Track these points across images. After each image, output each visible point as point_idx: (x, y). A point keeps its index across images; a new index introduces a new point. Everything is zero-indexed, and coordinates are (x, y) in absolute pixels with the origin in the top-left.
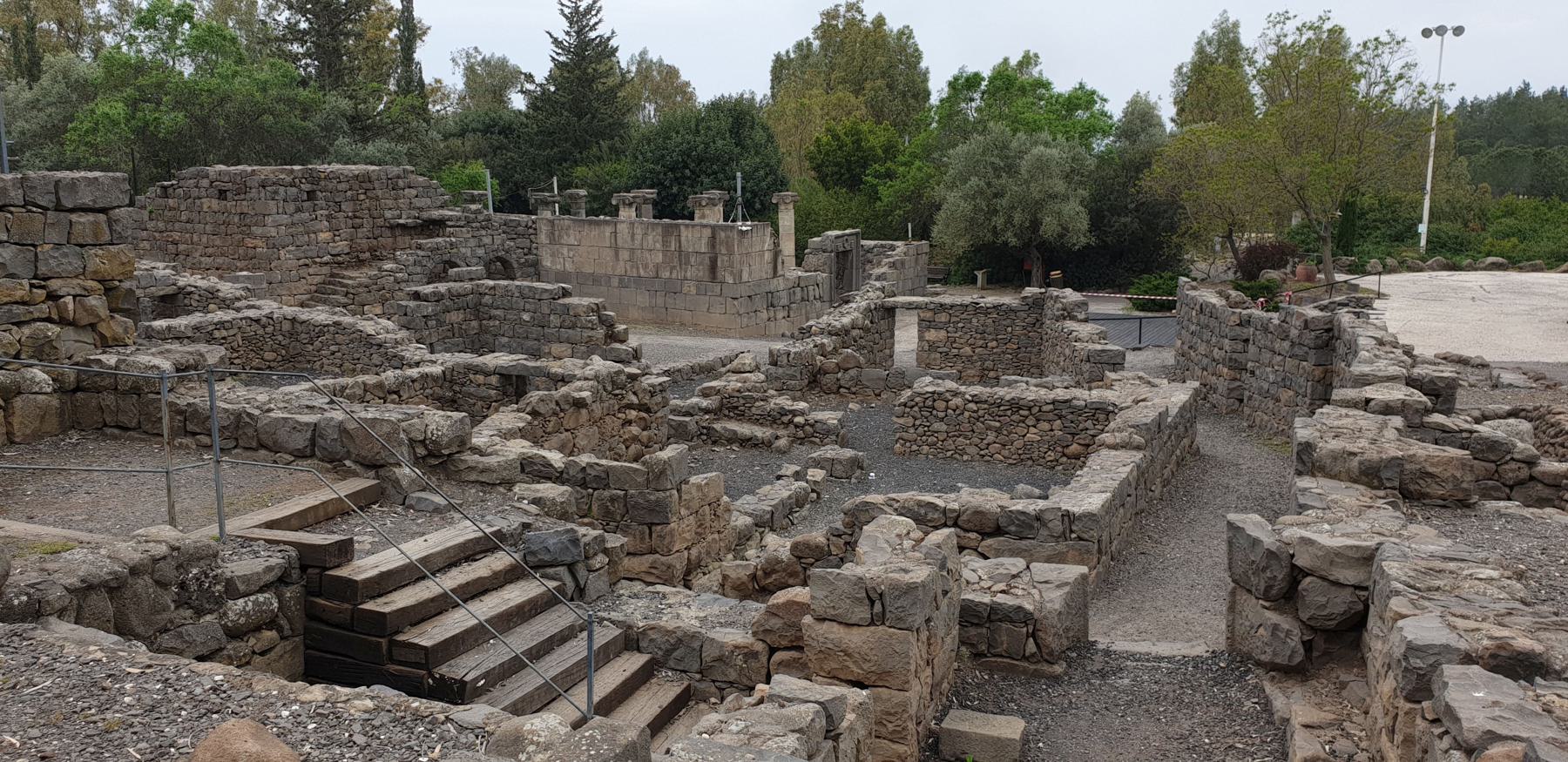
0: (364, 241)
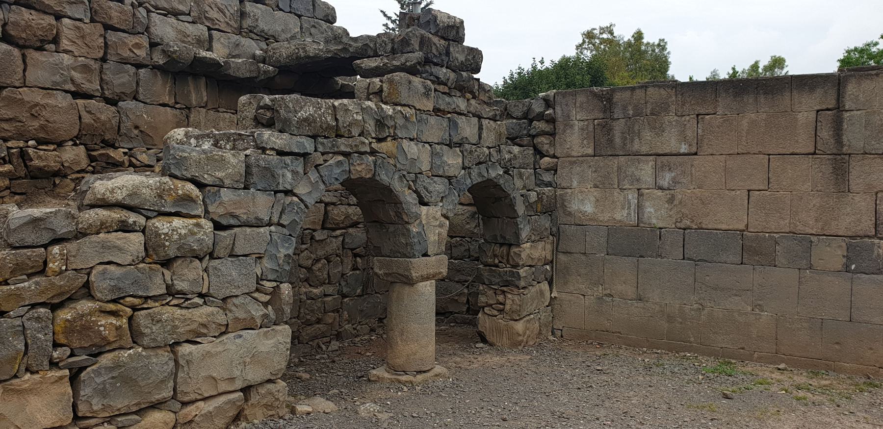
0: (62, 100)
